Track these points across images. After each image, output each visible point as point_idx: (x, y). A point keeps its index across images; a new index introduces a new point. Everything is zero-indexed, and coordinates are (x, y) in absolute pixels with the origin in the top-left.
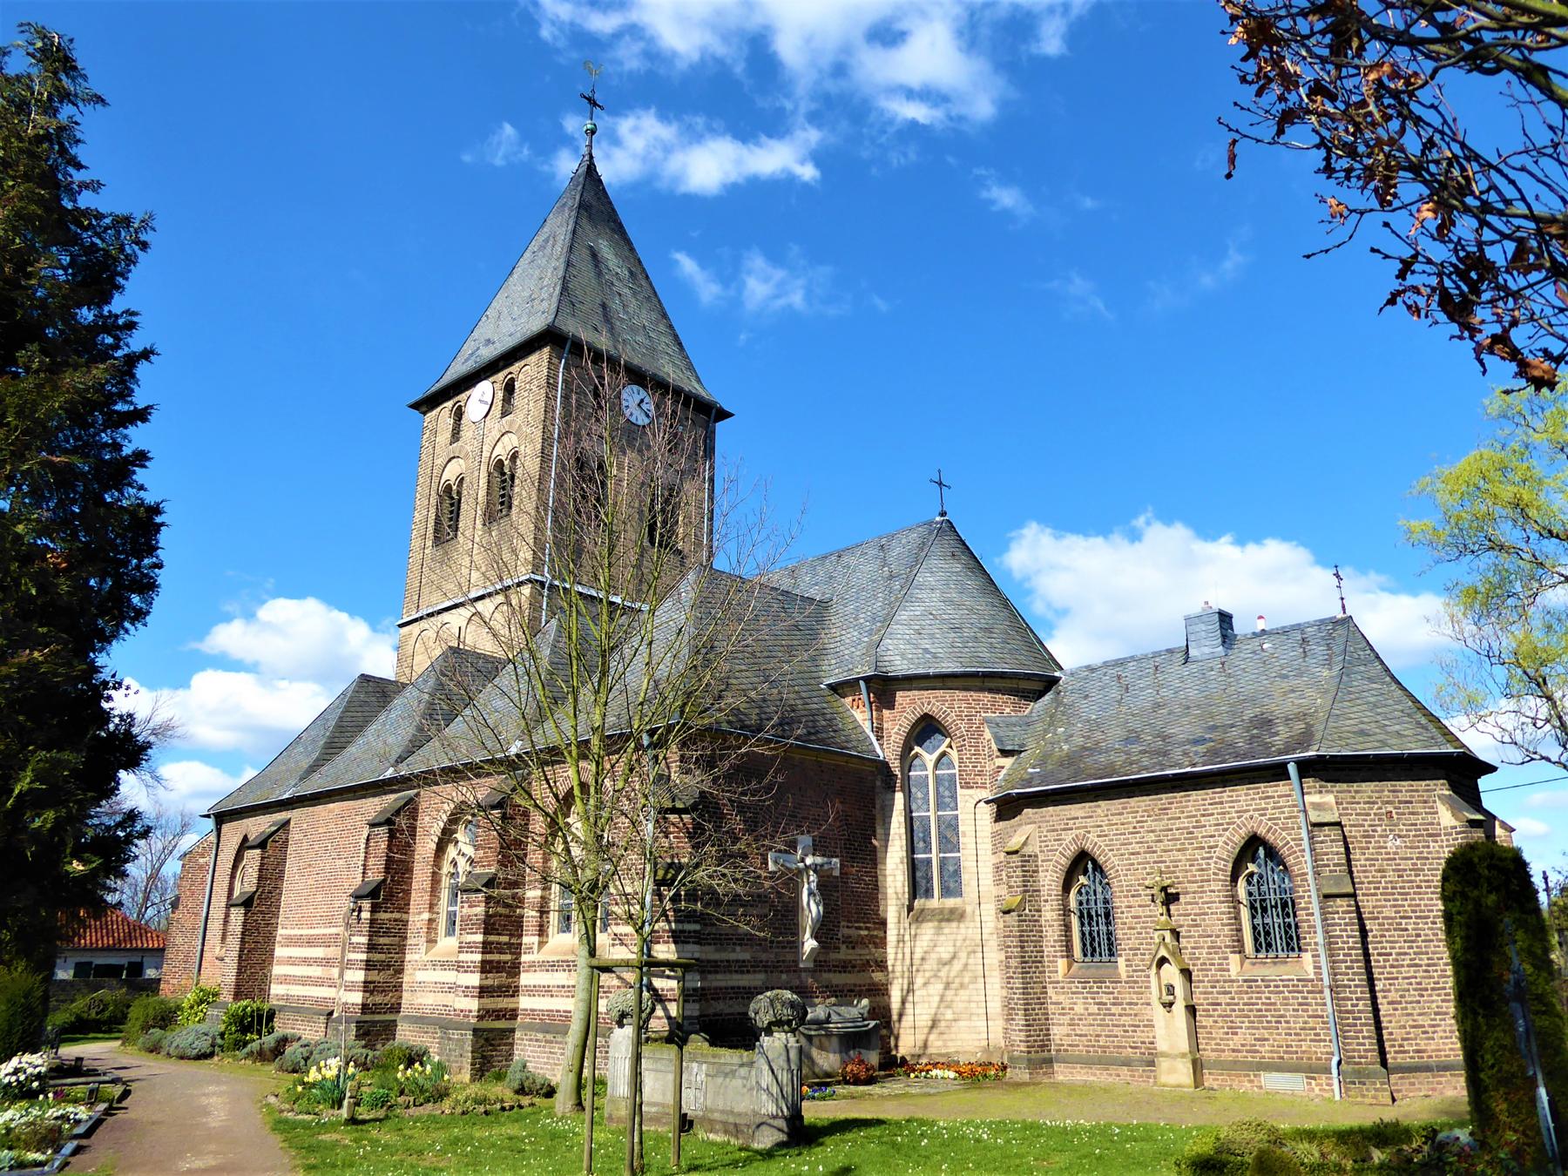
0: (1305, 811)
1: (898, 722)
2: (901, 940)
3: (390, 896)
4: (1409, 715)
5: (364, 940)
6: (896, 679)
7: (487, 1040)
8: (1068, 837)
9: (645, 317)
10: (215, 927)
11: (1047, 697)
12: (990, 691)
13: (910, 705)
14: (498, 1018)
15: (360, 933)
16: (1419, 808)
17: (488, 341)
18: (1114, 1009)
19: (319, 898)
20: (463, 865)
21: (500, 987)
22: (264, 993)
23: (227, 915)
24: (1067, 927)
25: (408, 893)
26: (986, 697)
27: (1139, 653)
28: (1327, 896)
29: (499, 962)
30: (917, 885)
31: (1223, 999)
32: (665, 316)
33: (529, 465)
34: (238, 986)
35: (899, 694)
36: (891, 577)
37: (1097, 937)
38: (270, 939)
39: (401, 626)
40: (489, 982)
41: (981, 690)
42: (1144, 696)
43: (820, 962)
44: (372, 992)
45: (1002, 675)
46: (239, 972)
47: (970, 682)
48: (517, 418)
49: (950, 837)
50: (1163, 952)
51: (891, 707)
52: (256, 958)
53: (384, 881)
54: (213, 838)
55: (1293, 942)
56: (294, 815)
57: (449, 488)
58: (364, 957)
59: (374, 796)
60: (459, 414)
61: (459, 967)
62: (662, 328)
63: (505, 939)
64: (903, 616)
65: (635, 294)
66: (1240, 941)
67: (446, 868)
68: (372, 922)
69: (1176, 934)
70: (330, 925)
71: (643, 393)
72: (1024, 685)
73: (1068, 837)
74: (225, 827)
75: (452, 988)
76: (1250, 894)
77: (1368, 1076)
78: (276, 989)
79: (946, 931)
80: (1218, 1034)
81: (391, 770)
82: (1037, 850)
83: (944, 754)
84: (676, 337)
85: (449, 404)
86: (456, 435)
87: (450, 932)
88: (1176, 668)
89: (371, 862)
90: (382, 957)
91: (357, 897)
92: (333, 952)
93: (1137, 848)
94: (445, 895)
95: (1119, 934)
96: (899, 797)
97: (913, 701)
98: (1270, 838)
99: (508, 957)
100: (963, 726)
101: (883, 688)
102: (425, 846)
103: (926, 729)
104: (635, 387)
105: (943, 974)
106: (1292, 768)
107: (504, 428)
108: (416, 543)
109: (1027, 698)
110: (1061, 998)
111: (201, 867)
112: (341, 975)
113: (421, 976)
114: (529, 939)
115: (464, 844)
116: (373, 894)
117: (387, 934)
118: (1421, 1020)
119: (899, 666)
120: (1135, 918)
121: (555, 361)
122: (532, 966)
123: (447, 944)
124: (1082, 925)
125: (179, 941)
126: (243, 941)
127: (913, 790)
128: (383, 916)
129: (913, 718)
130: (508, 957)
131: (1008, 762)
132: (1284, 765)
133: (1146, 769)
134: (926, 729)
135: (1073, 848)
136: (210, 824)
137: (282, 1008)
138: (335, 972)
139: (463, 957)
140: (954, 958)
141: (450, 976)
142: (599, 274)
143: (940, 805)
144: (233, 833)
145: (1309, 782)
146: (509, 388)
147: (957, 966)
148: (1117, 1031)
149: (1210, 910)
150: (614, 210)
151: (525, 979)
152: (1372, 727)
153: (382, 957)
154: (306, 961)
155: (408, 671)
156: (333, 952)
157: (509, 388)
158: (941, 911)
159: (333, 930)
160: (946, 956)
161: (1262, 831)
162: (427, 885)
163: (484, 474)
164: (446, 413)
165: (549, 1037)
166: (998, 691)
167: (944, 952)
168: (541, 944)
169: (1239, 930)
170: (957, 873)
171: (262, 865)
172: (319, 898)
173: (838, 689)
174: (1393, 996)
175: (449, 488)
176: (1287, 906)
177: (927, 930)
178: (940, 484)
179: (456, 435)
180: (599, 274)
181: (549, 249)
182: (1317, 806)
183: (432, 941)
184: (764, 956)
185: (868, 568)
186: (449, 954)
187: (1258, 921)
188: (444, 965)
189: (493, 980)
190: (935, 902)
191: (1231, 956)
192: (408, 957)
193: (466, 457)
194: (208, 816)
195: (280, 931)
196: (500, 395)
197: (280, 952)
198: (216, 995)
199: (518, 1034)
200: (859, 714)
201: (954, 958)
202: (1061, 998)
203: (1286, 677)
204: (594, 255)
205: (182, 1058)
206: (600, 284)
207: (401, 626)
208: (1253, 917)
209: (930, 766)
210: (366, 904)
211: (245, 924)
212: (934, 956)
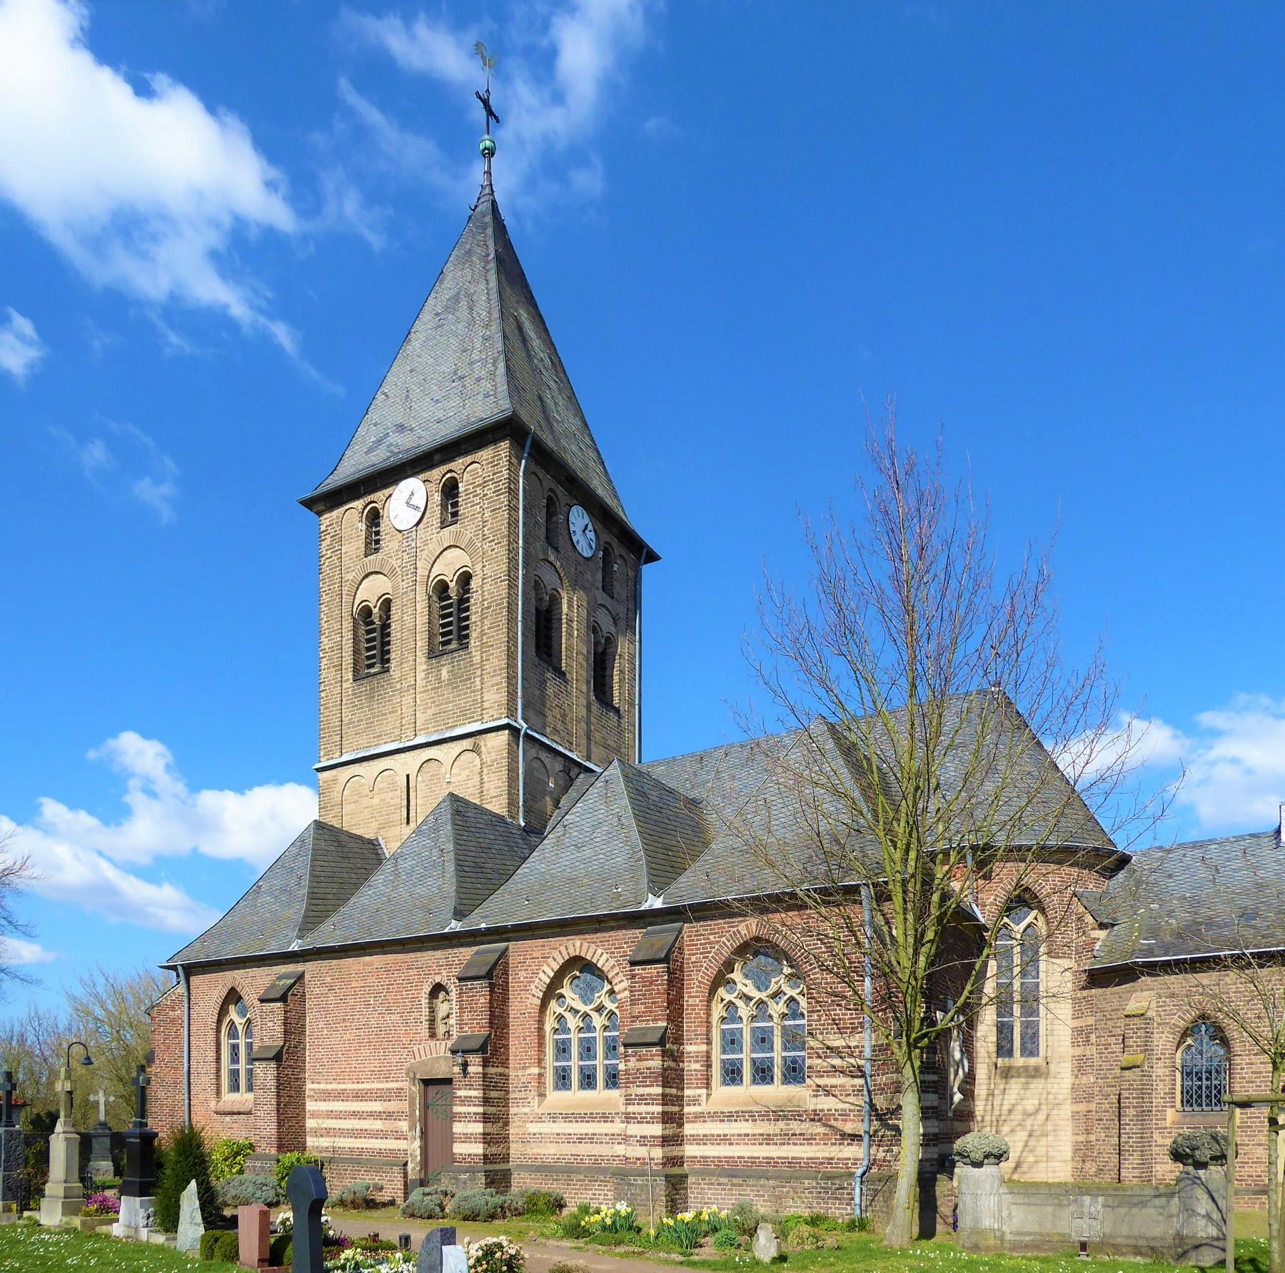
2: (991, 1094)
3: (495, 1051)
5: (477, 1093)
15: (470, 1087)
17: (401, 428)
25: (506, 1047)
30: (1004, 1048)
44: (489, 1143)
49: (1031, 1001)
53: (489, 1035)
59: (434, 949)
67: (550, 1024)
75: (591, 1138)
79: (1032, 1086)
94: (550, 1050)
102: (523, 1001)
105: (1029, 1122)
107: (443, 537)
113: (533, 1128)
128: (492, 1070)
140: (1037, 1111)
143: (1023, 973)
147: (1041, 1116)
157: (450, 490)
158: (1026, 1068)
160: (1030, 1108)
167: (1030, 1105)
170: (1035, 1035)
177: (1015, 1085)
183: (542, 1095)
190: (1018, 1060)
192: (512, 1110)
201: (1037, 1111)
212: (1019, 1108)
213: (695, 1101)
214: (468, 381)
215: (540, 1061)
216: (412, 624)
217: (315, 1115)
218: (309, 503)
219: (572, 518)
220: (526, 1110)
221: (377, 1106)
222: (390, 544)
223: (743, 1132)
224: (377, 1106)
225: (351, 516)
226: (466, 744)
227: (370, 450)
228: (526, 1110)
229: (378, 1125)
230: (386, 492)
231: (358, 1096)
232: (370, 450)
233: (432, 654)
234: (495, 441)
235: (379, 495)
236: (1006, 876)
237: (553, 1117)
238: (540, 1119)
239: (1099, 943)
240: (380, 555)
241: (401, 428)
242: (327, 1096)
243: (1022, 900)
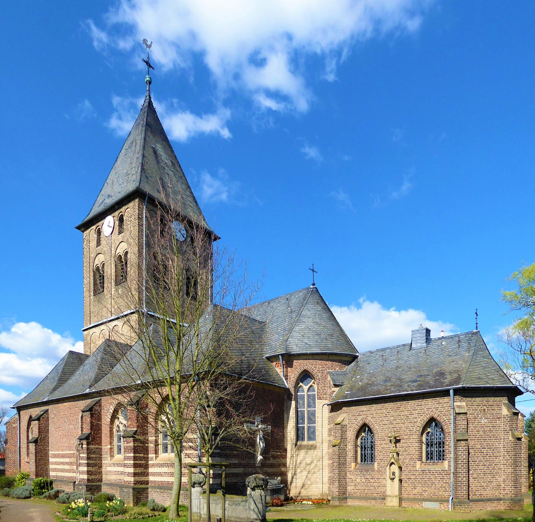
0: (454, 409)
1: (294, 373)
2: (292, 456)
3: (94, 439)
5: (85, 455)
6: (294, 355)
7: (138, 492)
8: (359, 418)
10: (24, 450)
11: (353, 364)
12: (331, 361)
14: (142, 484)
15: (83, 453)
17: (109, 196)
18: (371, 481)
19: (65, 440)
20: (122, 428)
21: (141, 473)
22: (47, 475)
23: (28, 446)
24: (356, 452)
25: (101, 438)
26: (329, 363)
27: (390, 345)
28: (458, 440)
29: (140, 464)
30: (299, 436)
31: (413, 477)
33: (133, 258)
34: (36, 472)
35: (295, 361)
36: (291, 312)
37: (367, 455)
38: (47, 455)
39: (84, 330)
40: (137, 471)
42: (393, 364)
43: (263, 464)
44: (90, 475)
45: (336, 354)
46: (36, 467)
48: (126, 234)
49: (312, 418)
50: (393, 461)
52: (42, 462)
53: (91, 433)
54: (17, 416)
55: (441, 457)
56: (50, 407)
57: (98, 269)
58: (86, 462)
59: (82, 400)
60: (99, 232)
61: (125, 466)
63: (142, 455)
64: (297, 328)
66: (421, 456)
68: (88, 449)
70: (70, 450)
72: (345, 359)
73: (359, 418)
74: (22, 412)
75: (122, 473)
76: (427, 440)
77: (463, 503)
78: (52, 474)
79: (309, 453)
80: (409, 489)
81: (88, 390)
82: (347, 423)
83: (311, 386)
85: (94, 227)
86: (99, 243)
87: (119, 452)
88: (406, 352)
89: (84, 426)
90: (93, 462)
91: (81, 439)
92: (73, 460)
94: (115, 439)
95: (376, 454)
96: (293, 403)
97: (300, 364)
98: (438, 419)
99: (144, 462)
101: (288, 359)
105: (307, 468)
106: (451, 392)
107: (118, 239)
108: (86, 294)
110: (352, 477)
111: (14, 428)
112: (77, 468)
113: (109, 469)
114: (151, 455)
115: (121, 419)
116: (87, 438)
117: (94, 453)
118: (483, 484)
119: (295, 350)
120: (383, 448)
122: (153, 465)
123: (119, 457)
124: (362, 451)
125: (10, 456)
126: (36, 456)
127: (299, 400)
128: (91, 446)
129: (300, 371)
130: (144, 462)
131: (336, 389)
132: (448, 391)
133: (393, 392)
134: (305, 376)
135: (361, 422)
136: (15, 411)
137: (55, 480)
138: (75, 467)
139: (126, 462)
140: (312, 462)
141: (121, 469)
143: (309, 406)
144: (25, 415)
145: (457, 397)
146: (121, 220)
147: (313, 465)
148: (371, 488)
149: (412, 445)
151: (151, 470)
152: (483, 376)
153: (93, 462)
154: (62, 463)
155: (89, 350)
156: (73, 460)
157: (121, 220)
158: (308, 446)
159: (72, 452)
160: (309, 462)
161: (435, 416)
162: (108, 434)
163: (113, 262)
164: (93, 232)
165: (162, 491)
166: (334, 361)
167: (308, 461)
168: (156, 457)
169: (422, 453)
170: (314, 432)
171: (39, 427)
172: (65, 440)
173: (270, 359)
174: (475, 476)
175: (98, 269)
176: (441, 444)
177: (302, 453)
178: (313, 270)
179: (99, 243)
180: (158, 162)
181: (134, 147)
182: (459, 407)
183: (112, 456)
184: (243, 462)
185: (281, 308)
186: (120, 461)
187: (429, 449)
188: (118, 465)
189: (139, 470)
190: (306, 442)
191: (418, 462)
192: (103, 462)
193: (104, 254)
194: (14, 408)
195: (50, 452)
196: (117, 223)
197: (51, 460)
198: (28, 475)
199: (149, 490)
200: (279, 370)
201: (312, 462)
202: (352, 477)
203: (451, 356)
205: (18, 498)
207: (84, 330)
208: (427, 448)
209: (306, 391)
210: (85, 442)
211: (36, 449)
212: (304, 462)
213: (152, 459)
214: (130, 176)
215: (111, 443)
216: (110, 271)
217: (52, 464)
218: (79, 228)
220: (107, 462)
221: (67, 460)
222: (103, 242)
223: (165, 471)
224: (67, 460)
225: (92, 232)
226: (125, 319)
227: (100, 205)
228: (107, 462)
229: (67, 467)
230: (102, 222)
231: (63, 456)
232: (100, 205)
233: (116, 285)
234: (134, 199)
235: (100, 223)
236: (299, 366)
237: (114, 465)
238: (110, 466)
239: (335, 393)
240: (101, 247)
241: (109, 196)
242: (56, 456)
243: (305, 376)
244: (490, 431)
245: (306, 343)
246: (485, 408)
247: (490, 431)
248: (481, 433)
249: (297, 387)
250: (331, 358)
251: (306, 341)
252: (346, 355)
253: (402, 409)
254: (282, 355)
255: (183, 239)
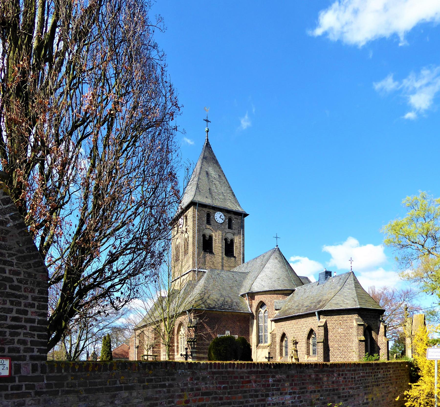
1: (255, 303)
4: (353, 298)
6: (254, 293)
8: (281, 329)
9: (223, 189)
12: (276, 294)
13: (258, 298)
16: (349, 321)
32: (230, 187)
41: (274, 294)
45: (279, 290)
47: (269, 293)
50: (292, 355)
51: (254, 300)
62: (228, 191)
65: (220, 182)
68: (153, 351)
69: (297, 351)
71: (221, 214)
72: (285, 292)
73: (281, 329)
83: (266, 310)
84: (233, 193)
93: (292, 332)
97: (258, 298)
100: (269, 303)
101: (252, 295)
103: (262, 304)
104: (219, 212)
109: (286, 295)
114: (176, 353)
119: (255, 289)
121: (195, 210)
129: (258, 302)
131: (277, 312)
134: (262, 304)
142: (209, 179)
150: (215, 156)
166: (278, 294)
173: (243, 296)
200: (246, 301)
204: (207, 173)
206: (209, 182)
209: (263, 313)
219: (215, 215)
244: (345, 336)
245: (262, 285)
246: (341, 322)
247: (345, 336)
248: (338, 337)
249: (257, 311)
250: (276, 292)
251: (263, 283)
252: (287, 290)
253: (299, 324)
254: (248, 293)
255: (223, 221)
